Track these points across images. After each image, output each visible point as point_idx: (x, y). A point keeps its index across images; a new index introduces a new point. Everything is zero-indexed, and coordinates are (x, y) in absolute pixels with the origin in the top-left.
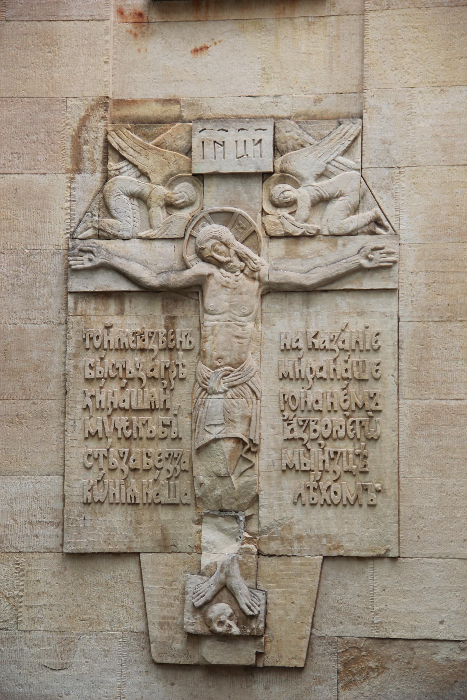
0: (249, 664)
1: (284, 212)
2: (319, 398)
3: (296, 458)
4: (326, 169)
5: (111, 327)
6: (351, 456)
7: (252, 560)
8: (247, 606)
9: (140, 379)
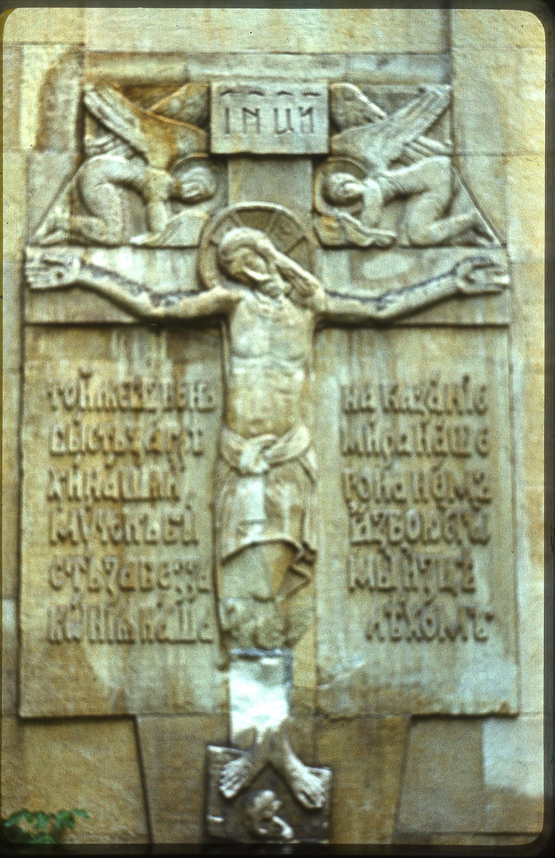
1: (344, 214)
3: (370, 569)
4: (404, 154)
9: (135, 454)
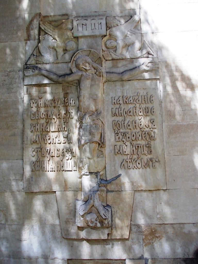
0: (105, 239)
2: (130, 123)
5: (42, 98)
6: (145, 147)
7: (104, 195)
8: (104, 214)
